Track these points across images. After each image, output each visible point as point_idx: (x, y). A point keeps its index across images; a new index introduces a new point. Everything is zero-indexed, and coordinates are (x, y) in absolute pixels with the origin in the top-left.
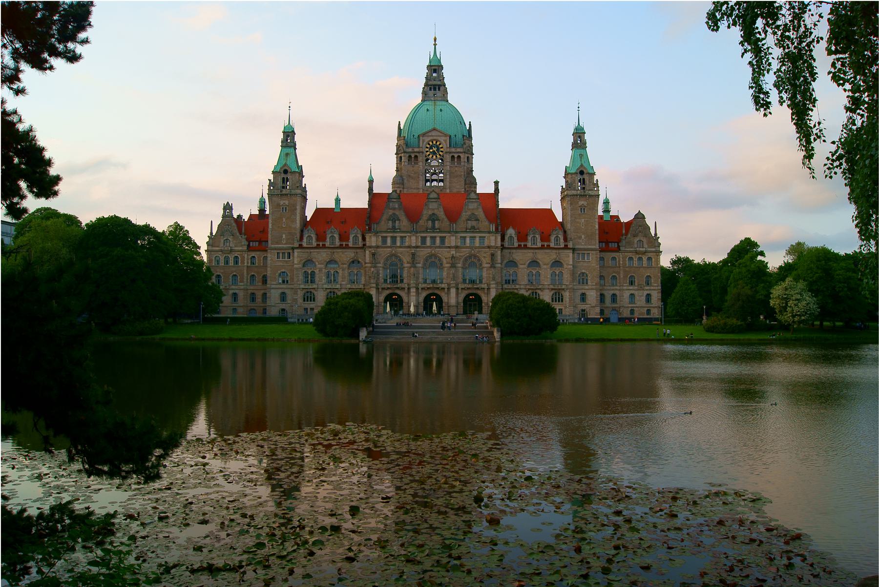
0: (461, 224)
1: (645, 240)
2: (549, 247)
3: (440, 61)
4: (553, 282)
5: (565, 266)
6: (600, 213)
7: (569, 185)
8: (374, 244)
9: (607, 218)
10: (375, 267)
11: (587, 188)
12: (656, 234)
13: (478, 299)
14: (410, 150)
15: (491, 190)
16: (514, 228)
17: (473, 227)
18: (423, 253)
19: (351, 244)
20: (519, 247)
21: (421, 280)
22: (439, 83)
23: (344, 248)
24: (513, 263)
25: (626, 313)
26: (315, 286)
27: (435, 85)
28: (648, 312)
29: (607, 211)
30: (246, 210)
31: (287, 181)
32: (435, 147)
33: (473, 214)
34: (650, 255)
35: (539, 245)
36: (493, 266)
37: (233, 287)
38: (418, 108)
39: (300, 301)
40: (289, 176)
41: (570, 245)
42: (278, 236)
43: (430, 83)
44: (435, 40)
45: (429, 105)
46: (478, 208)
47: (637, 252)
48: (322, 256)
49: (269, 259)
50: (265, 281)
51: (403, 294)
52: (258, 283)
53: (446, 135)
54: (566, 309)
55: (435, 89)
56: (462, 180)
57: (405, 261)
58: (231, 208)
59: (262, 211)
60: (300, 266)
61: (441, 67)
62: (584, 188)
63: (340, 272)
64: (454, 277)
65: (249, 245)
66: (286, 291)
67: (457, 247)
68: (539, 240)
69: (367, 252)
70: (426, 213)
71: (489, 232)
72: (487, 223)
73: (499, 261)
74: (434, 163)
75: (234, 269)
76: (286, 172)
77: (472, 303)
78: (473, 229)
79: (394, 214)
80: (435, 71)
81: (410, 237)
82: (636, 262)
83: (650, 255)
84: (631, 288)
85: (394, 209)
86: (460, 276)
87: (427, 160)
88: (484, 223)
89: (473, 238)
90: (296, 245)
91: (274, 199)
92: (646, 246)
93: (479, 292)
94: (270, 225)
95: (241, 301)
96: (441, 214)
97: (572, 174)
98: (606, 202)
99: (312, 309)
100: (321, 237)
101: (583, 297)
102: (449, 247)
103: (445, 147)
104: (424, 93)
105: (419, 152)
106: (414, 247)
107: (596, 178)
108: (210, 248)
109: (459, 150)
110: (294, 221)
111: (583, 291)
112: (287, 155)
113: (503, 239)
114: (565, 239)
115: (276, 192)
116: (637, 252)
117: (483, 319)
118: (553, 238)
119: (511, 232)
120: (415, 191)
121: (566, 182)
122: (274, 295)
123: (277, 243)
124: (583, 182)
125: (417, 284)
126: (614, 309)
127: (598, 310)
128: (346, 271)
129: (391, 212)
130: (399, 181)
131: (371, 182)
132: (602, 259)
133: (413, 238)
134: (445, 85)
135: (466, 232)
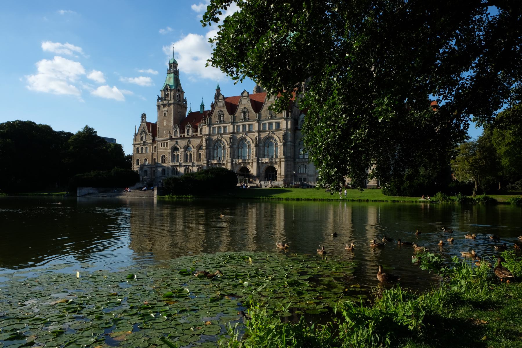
48: (182, 143)
58: (145, 117)
70: (240, 108)
75: (145, 155)
85: (220, 107)
86: (262, 153)
90: (169, 137)
96: (250, 107)
100: (182, 131)
106: (231, 133)
110: (170, 121)
123: (161, 137)
135: (266, 120)
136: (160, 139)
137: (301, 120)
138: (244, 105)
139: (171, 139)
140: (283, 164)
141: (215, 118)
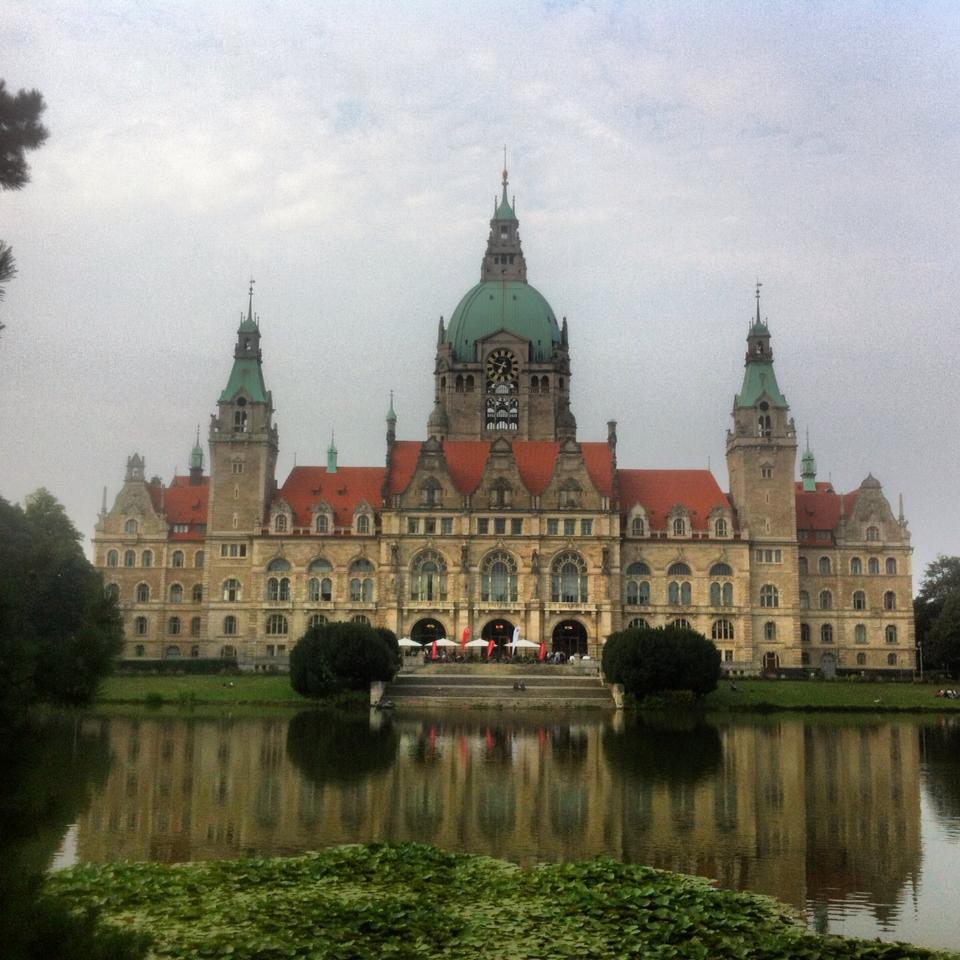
0: (551, 499)
1: (881, 527)
2: (706, 540)
3: (512, 212)
4: (714, 602)
5: (736, 573)
6: (798, 478)
7: (742, 430)
8: (395, 531)
9: (809, 486)
10: (397, 571)
11: (774, 433)
12: (902, 518)
13: (580, 631)
14: (459, 366)
15: (602, 437)
16: (643, 506)
17: (571, 503)
18: (482, 548)
19: (354, 531)
20: (653, 539)
21: (477, 596)
22: (512, 251)
23: (342, 538)
24: (641, 568)
25: (850, 662)
26: (288, 606)
27: (504, 252)
28: (892, 659)
29: (809, 475)
30: (168, 465)
31: (245, 416)
32: (503, 363)
33: (571, 480)
34: (892, 554)
35: (689, 534)
36: (606, 572)
37: (140, 606)
38: (474, 293)
39: (261, 632)
40: (248, 410)
41: (745, 535)
42: (226, 516)
43: (495, 251)
44: (505, 175)
45: (494, 288)
46: (578, 470)
47: (867, 550)
48: (300, 553)
49: (207, 556)
50: (197, 595)
51: (446, 621)
52: (185, 599)
53: (523, 341)
54: (739, 652)
55: (504, 261)
56: (551, 419)
57: (450, 562)
59: (196, 471)
60: (263, 569)
61: (515, 223)
62: (768, 434)
63: (334, 580)
64: (538, 592)
65: (171, 533)
66: (237, 614)
67: (541, 538)
68: (687, 526)
69: (384, 546)
71: (600, 512)
72: (595, 496)
73: (617, 563)
74: (503, 389)
75: (142, 574)
76: (242, 402)
77: (569, 637)
78: (572, 507)
79: (432, 478)
80: (504, 229)
81: (459, 518)
82: (865, 568)
83: (892, 554)
84: (858, 614)
85: (433, 469)
86: (548, 589)
87: (489, 384)
88: (591, 497)
89: (570, 523)
90: (257, 531)
91: (221, 449)
92: (883, 537)
93: (582, 620)
94: (212, 497)
95: (153, 631)
96: (514, 479)
97: (746, 408)
98: (809, 459)
99: (282, 647)
101: (770, 629)
102: (529, 538)
103: (521, 362)
104: (487, 269)
105: (475, 371)
106: (466, 537)
107: (789, 415)
108: (102, 536)
109: (545, 367)
111: (770, 619)
112: (245, 372)
113: (623, 525)
114: (736, 526)
115: (228, 437)
116: (867, 550)
117: (588, 662)
118: (712, 523)
119: (638, 511)
120: (469, 438)
121: (737, 423)
122: (214, 622)
123: (223, 528)
124: (766, 422)
125: (471, 604)
126: (827, 653)
127: (798, 653)
128: (345, 579)
129: (426, 475)
130: (442, 421)
131: (392, 421)
132: (803, 560)
133: (466, 521)
134: (521, 254)
135: (558, 511)
136: (215, 533)
137: (634, 517)
138: (501, 471)
139: (265, 535)
140: (606, 619)
141: (414, 498)
